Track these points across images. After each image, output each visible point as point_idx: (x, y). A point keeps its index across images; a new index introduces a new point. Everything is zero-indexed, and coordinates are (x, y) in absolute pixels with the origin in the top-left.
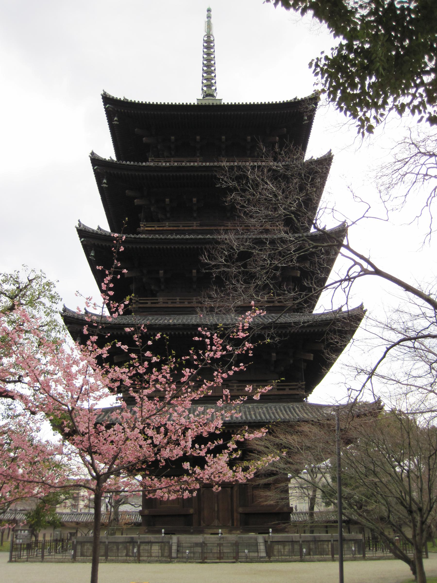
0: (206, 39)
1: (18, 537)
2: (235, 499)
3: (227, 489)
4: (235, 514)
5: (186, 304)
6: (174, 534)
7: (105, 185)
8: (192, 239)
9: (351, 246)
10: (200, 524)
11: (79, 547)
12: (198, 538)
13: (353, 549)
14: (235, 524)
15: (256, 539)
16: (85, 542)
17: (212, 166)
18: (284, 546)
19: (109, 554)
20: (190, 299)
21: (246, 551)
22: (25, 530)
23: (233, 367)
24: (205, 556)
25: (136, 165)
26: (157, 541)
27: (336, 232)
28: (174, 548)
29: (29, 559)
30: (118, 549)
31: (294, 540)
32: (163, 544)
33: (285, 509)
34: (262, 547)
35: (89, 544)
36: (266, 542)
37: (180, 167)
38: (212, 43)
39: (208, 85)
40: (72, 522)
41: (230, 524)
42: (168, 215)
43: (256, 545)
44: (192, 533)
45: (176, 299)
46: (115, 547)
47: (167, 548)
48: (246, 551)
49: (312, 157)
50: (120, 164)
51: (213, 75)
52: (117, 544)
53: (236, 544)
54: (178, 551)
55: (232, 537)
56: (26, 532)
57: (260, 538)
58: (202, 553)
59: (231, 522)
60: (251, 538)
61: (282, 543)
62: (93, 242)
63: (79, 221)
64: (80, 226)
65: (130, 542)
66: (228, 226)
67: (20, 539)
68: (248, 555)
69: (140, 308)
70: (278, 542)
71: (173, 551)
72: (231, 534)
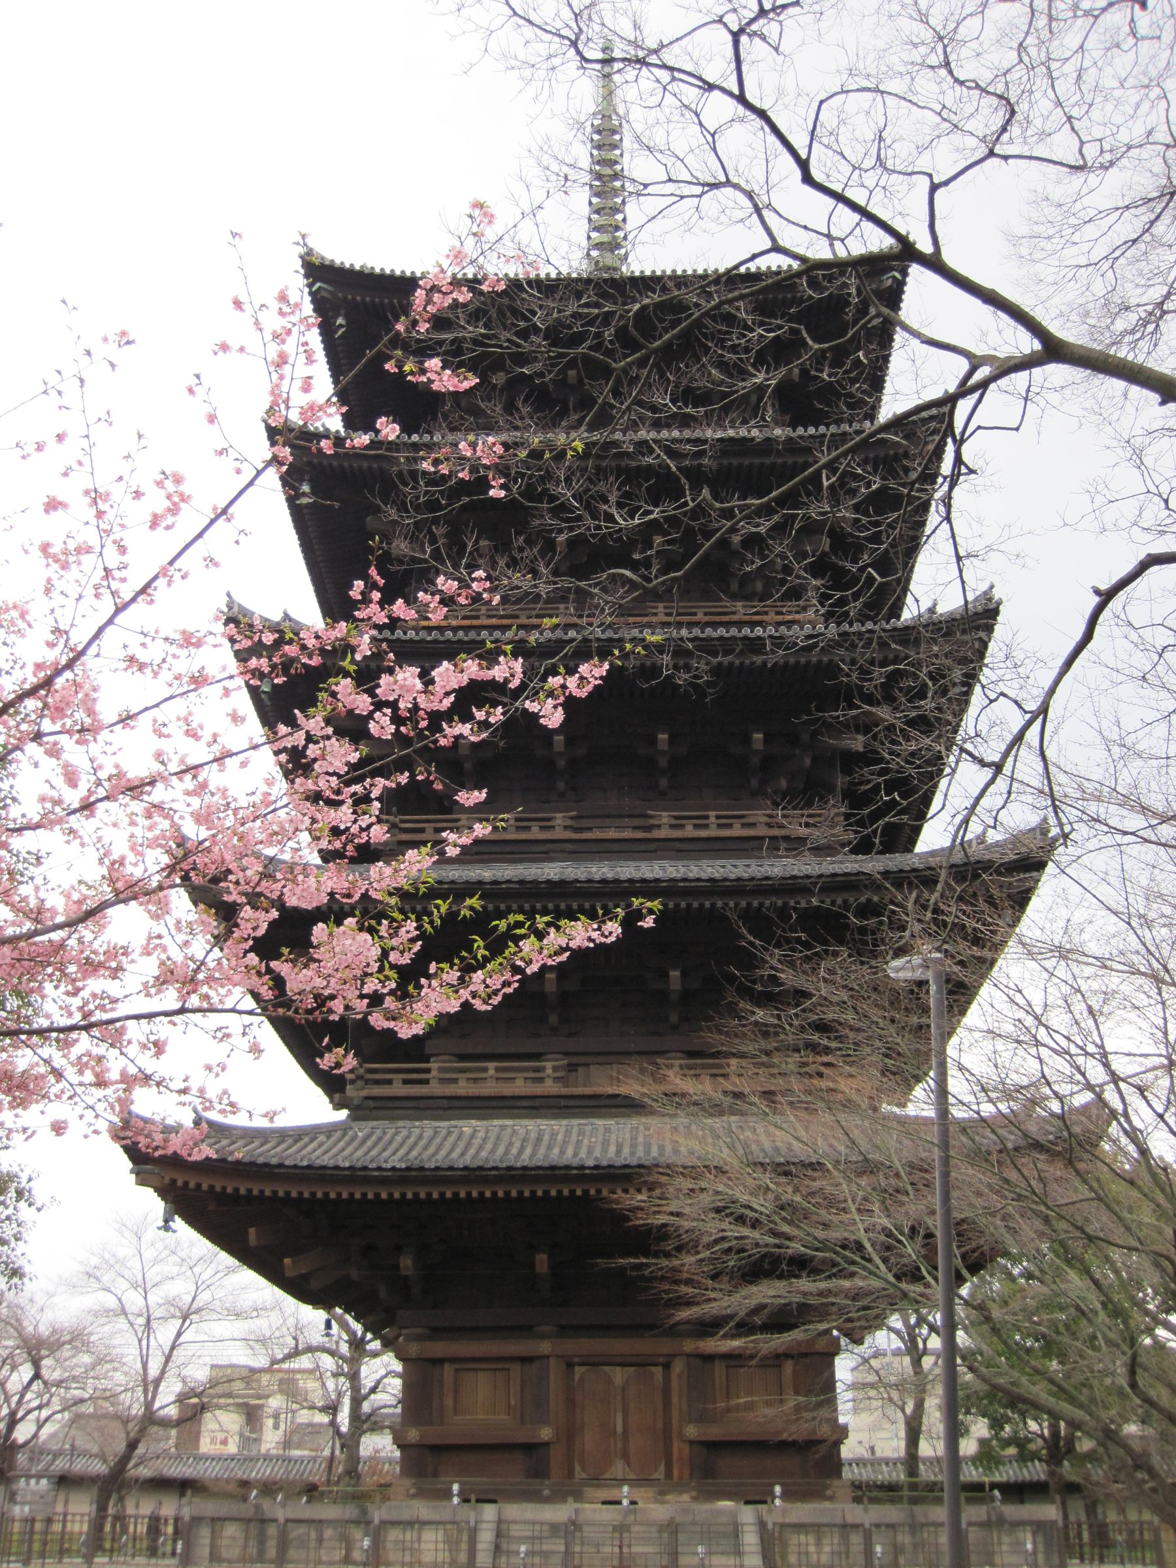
0: (596, 122)
1: (18, 1498)
2: (675, 1400)
3: (653, 1369)
4: (676, 1446)
5: (535, 833)
6: (495, 1502)
7: (305, 501)
9: (950, 258)
10: (570, 1474)
11: (204, 1534)
12: (559, 1513)
13: (1029, 1546)
14: (676, 1473)
15: (734, 1515)
18: (819, 1543)
19: (292, 1553)
20: (549, 819)
21: (700, 1549)
23: (441, 580)
28: (486, 1537)
30: (320, 1540)
31: (850, 1519)
32: (449, 1526)
33: (824, 1431)
34: (750, 1539)
36: (762, 1524)
39: (602, 243)
40: (227, 1481)
41: (660, 1474)
43: (736, 1533)
44: (547, 1500)
46: (313, 1535)
47: (465, 1537)
48: (700, 1549)
51: (619, 217)
52: (319, 1523)
53: (672, 1529)
54: (497, 1549)
55: (658, 1511)
56: (44, 1481)
57: (747, 1514)
58: (568, 1553)
59: (662, 1468)
60: (720, 1512)
61: (816, 1529)
63: (228, 595)
64: (230, 608)
65: (357, 1522)
67: (23, 1503)
68: (707, 1562)
70: (800, 1527)
71: (480, 1546)
72: (663, 1502)
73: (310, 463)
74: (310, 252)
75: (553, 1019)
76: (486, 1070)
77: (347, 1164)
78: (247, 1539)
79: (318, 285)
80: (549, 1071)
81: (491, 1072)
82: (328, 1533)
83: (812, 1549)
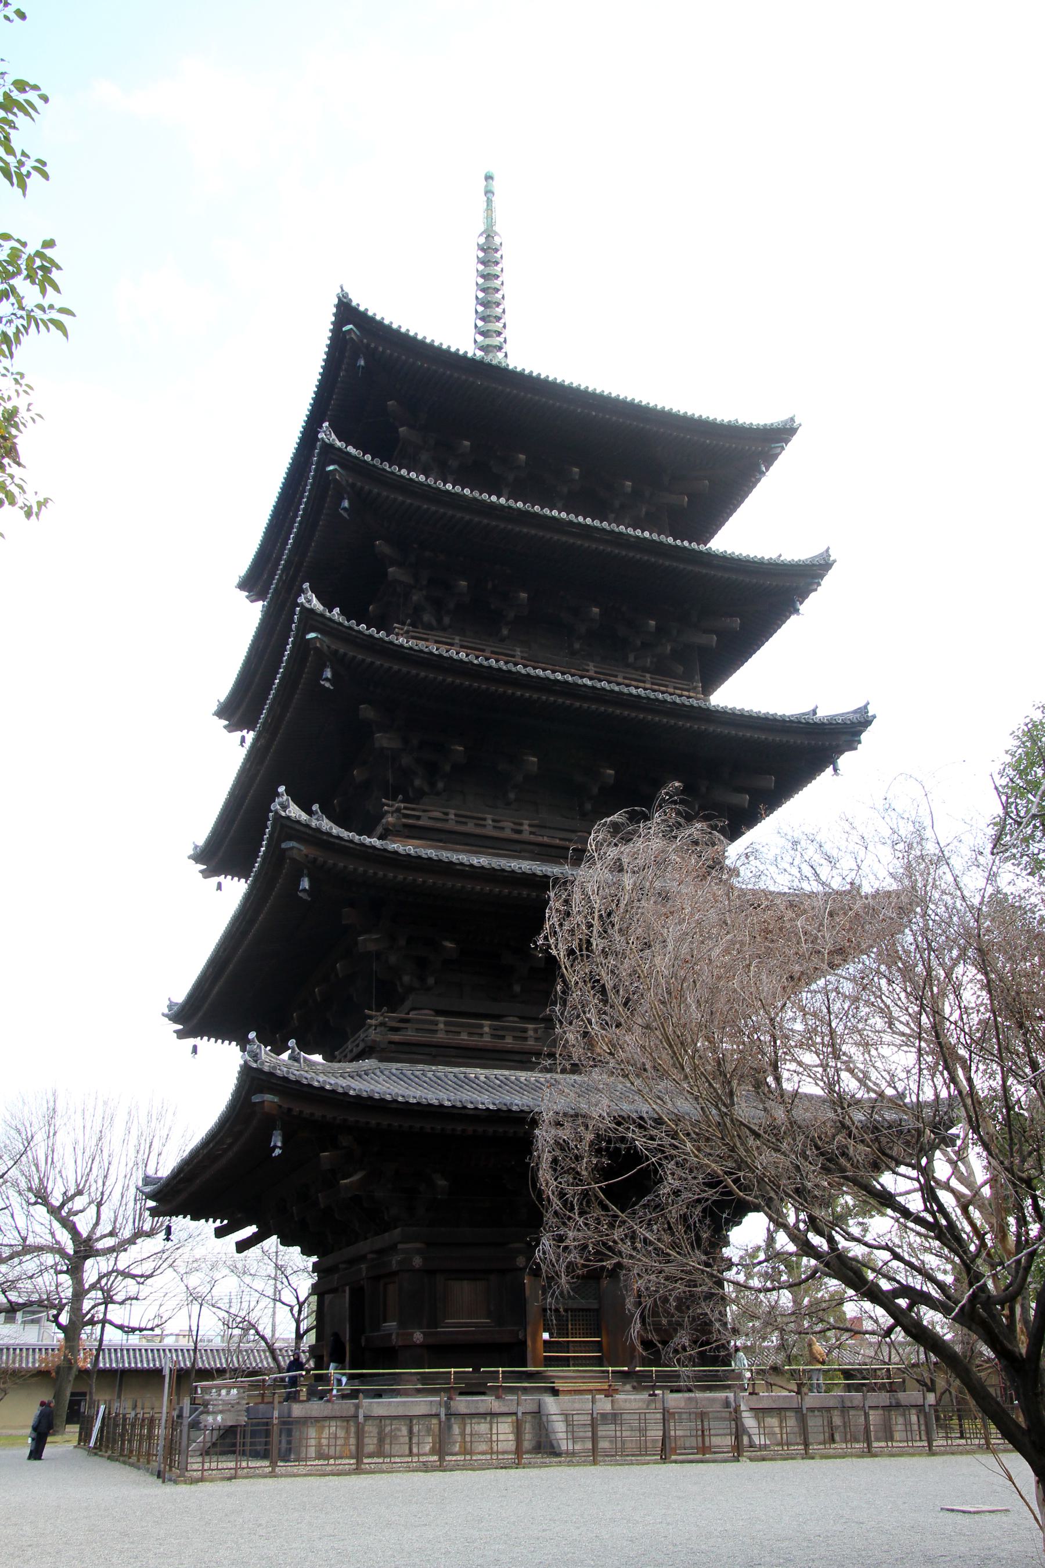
1: (211, 1408)
8: (566, 682)
16: (326, 1418)
17: (596, 528)
22: (229, 1388)
24: (673, 1445)
25: (429, 486)
26: (504, 1409)
27: (852, 723)
29: (240, 1472)
35: (333, 1423)
37: (528, 512)
38: (496, 250)
42: (447, 620)
45: (485, 819)
46: (404, 1431)
49: (780, 556)
50: (392, 473)
52: (410, 1419)
56: (234, 1391)
62: (333, 647)
66: (588, 671)
67: (213, 1413)
69: (405, 825)
73: (353, 486)
74: (346, 296)
75: (517, 988)
76: (481, 1026)
77: (450, 1104)
78: (347, 1438)
79: (351, 326)
80: (531, 1033)
81: (486, 1029)
82: (415, 1429)
83: (777, 1430)
